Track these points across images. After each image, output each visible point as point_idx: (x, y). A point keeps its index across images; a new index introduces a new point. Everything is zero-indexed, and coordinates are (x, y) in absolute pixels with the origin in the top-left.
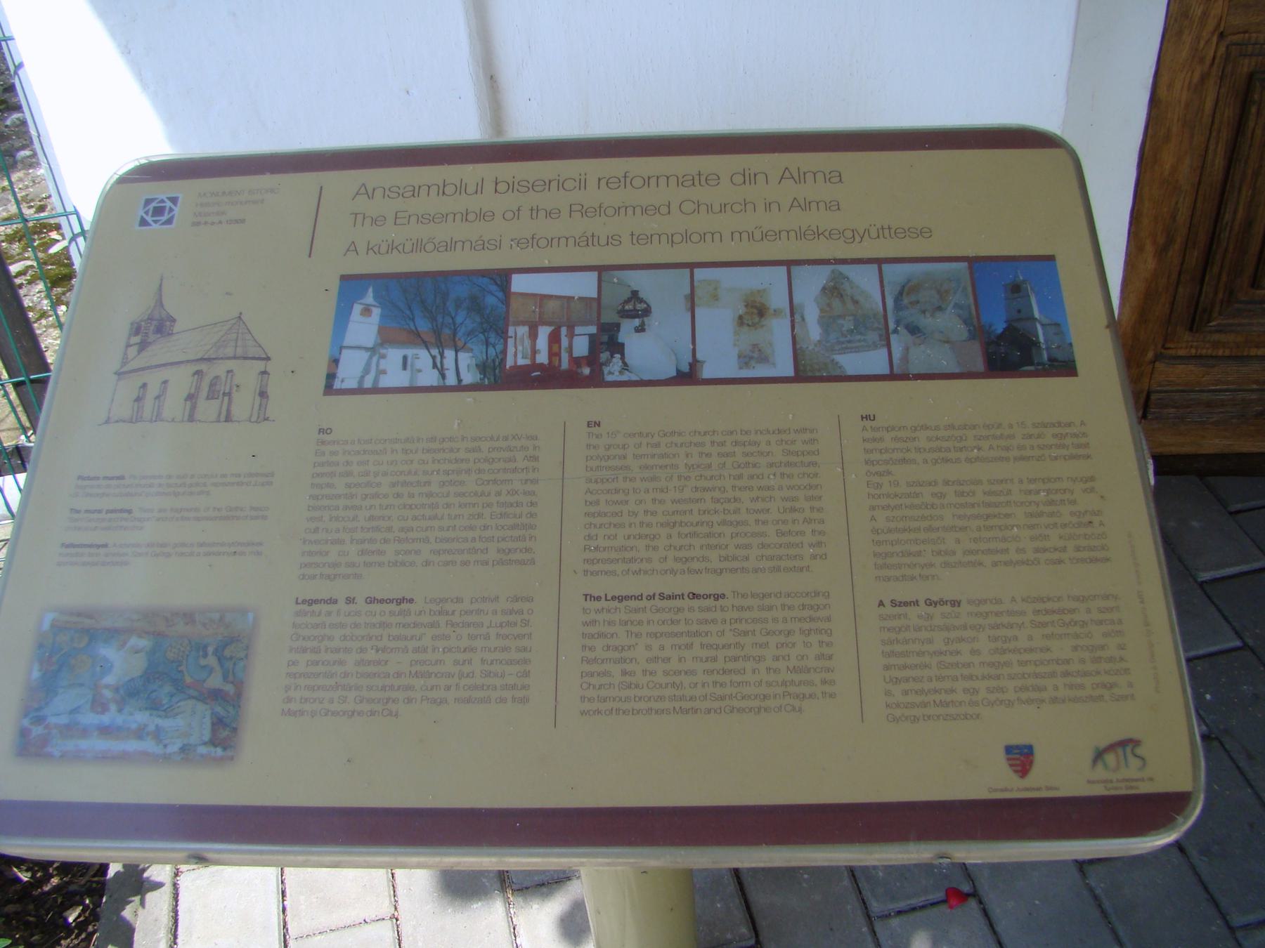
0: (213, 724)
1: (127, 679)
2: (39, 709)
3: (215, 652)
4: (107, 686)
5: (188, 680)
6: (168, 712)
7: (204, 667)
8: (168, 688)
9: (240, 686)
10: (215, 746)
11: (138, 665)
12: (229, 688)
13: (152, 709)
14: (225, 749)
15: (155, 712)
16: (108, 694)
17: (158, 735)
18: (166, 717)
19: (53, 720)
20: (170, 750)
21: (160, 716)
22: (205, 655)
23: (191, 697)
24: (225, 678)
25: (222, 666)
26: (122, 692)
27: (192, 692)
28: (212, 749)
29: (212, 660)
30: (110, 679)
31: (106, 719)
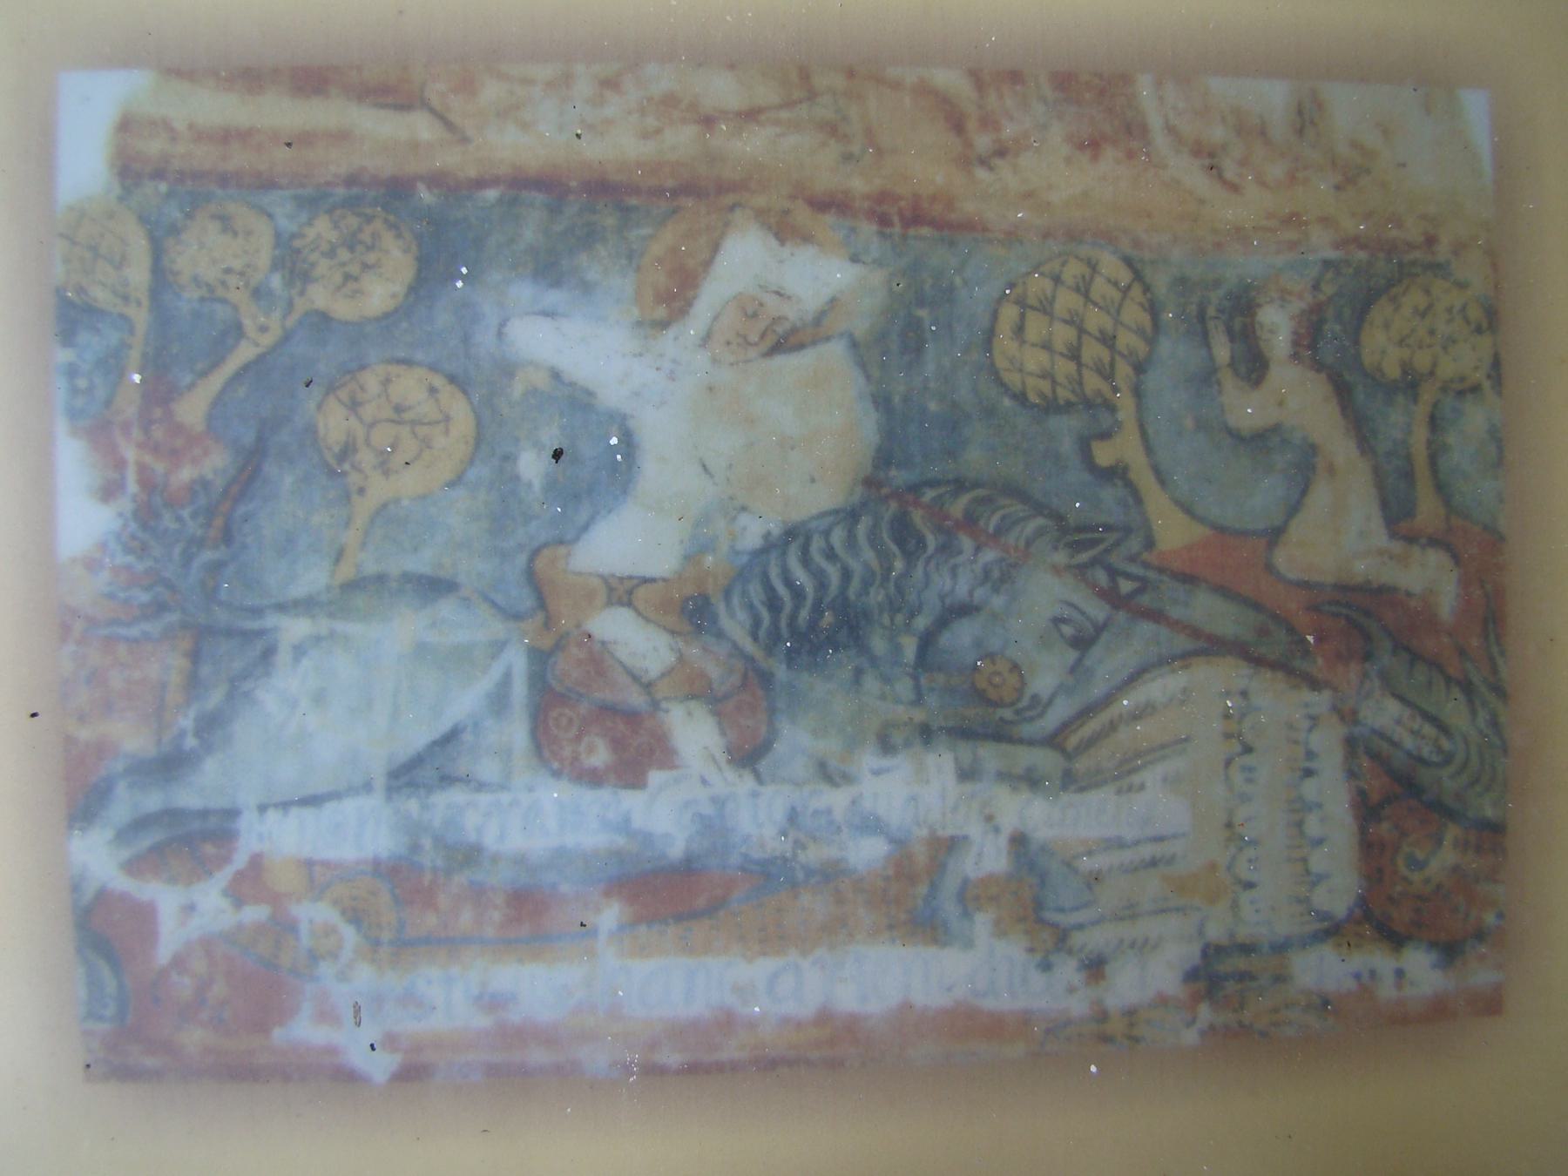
1: (753, 531)
3: (1309, 339)
4: (623, 591)
5: (1173, 532)
7: (1260, 442)
9: (1483, 553)
10: (1395, 939)
12: (1430, 578)
13: (964, 733)
15: (990, 755)
16: (638, 643)
18: (1069, 781)
21: (1031, 780)
23: (1212, 646)
24: (1396, 513)
25: (1361, 428)
27: (1208, 610)
28: (1381, 960)
30: (629, 540)
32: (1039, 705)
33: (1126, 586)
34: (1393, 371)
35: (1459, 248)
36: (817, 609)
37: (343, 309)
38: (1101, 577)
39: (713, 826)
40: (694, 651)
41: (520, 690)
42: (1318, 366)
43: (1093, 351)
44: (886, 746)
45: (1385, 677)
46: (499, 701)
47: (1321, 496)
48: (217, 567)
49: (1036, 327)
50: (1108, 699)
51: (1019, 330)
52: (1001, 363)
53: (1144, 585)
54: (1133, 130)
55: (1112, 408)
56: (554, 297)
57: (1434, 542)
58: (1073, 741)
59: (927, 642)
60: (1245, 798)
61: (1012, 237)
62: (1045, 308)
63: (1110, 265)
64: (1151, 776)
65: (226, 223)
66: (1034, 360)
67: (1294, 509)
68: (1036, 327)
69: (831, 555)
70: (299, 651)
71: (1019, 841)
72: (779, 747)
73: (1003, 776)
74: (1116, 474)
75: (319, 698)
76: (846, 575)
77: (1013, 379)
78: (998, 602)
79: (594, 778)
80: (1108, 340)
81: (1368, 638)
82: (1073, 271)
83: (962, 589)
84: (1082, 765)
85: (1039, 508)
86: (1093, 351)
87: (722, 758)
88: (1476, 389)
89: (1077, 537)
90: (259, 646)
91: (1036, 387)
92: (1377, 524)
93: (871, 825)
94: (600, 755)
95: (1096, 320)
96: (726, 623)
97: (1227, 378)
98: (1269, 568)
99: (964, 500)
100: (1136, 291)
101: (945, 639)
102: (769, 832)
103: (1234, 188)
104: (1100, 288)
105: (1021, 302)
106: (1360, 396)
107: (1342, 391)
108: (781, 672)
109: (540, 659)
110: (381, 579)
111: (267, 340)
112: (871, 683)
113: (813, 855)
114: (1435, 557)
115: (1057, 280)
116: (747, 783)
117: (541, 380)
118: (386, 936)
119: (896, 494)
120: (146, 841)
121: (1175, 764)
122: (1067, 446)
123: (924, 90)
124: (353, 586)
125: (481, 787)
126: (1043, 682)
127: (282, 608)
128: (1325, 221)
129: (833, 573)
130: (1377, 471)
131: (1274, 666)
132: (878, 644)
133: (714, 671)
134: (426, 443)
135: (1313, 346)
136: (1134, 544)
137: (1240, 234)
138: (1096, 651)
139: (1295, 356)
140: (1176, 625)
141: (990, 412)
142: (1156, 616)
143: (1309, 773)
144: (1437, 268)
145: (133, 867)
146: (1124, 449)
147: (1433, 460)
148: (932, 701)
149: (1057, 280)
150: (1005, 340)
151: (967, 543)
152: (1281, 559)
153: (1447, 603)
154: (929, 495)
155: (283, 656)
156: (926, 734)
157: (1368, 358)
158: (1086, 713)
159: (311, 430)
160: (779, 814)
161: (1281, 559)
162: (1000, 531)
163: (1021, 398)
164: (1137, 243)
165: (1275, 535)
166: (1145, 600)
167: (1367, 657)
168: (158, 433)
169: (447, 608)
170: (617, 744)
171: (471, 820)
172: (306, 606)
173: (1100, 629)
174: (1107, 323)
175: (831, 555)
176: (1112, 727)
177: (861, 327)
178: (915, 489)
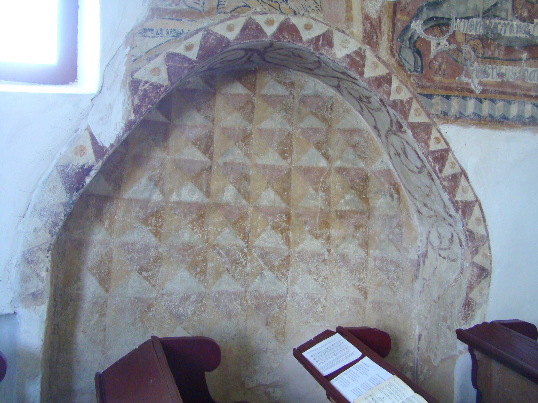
19: (459, 26)
94: (525, 14)
118: (480, 55)
120: (432, 23)
125: (502, 19)
145: (426, 31)
170: (529, 11)
171: (499, 27)
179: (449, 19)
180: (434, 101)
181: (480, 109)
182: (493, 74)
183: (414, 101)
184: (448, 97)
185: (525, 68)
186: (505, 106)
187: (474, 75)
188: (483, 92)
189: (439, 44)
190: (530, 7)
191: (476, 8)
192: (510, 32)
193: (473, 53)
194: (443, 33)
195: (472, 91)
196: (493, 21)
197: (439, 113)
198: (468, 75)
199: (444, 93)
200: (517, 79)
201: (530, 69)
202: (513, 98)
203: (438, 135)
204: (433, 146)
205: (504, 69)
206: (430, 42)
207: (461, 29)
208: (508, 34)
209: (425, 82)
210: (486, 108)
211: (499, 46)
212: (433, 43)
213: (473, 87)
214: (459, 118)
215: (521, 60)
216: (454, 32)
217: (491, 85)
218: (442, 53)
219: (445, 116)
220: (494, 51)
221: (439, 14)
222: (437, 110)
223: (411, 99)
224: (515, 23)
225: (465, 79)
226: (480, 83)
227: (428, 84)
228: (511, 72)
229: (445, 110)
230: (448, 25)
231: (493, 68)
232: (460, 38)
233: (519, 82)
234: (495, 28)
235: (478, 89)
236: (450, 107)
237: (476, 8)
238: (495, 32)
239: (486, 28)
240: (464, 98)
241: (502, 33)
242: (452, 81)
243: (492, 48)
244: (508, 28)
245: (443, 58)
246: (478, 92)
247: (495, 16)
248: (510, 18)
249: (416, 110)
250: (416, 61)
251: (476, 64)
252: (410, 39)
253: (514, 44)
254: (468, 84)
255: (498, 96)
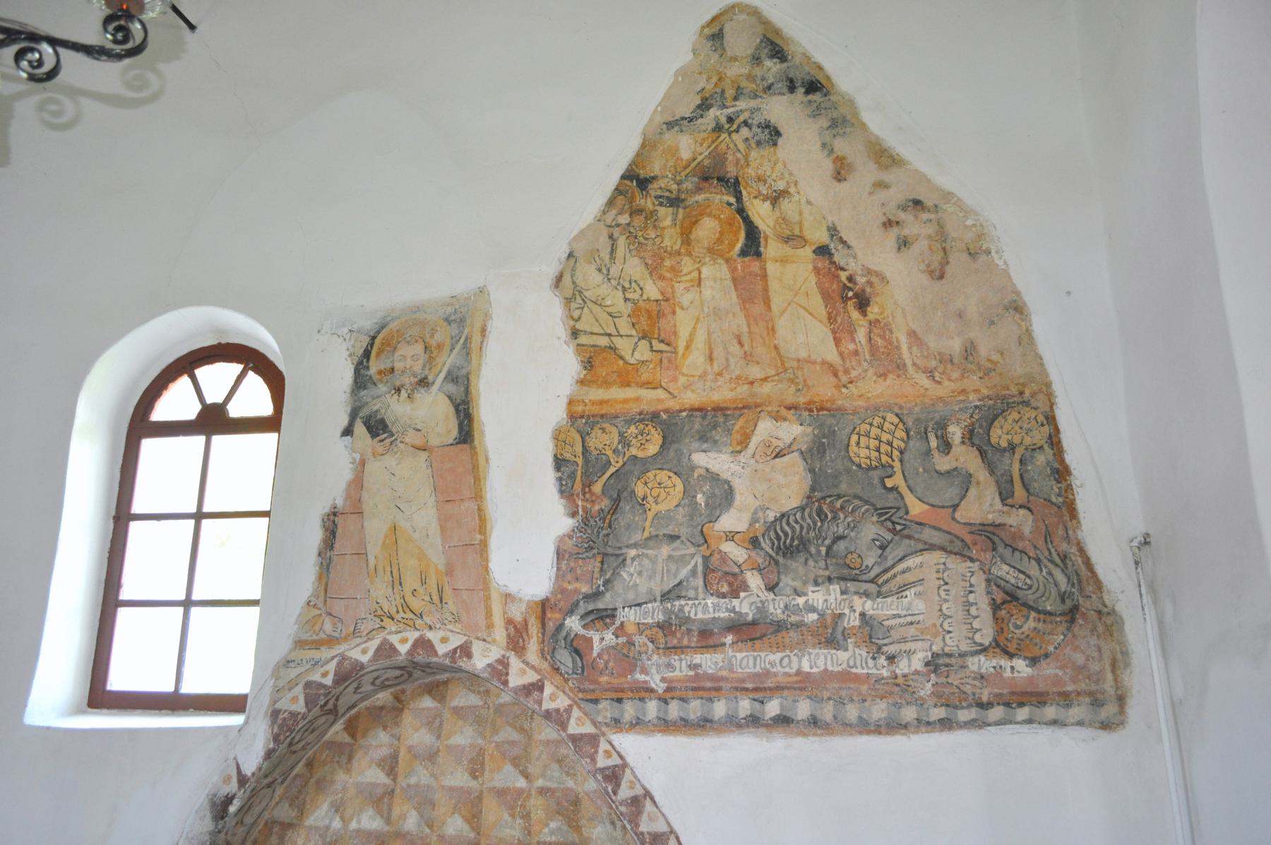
0: (996, 607)
1: (771, 516)
2: (597, 595)
3: (970, 436)
4: (730, 536)
5: (916, 508)
6: (878, 586)
8: (871, 530)
11: (788, 487)
12: (1021, 520)
13: (842, 579)
14: (1033, 661)
16: (737, 553)
17: (871, 633)
19: (629, 616)
20: (903, 667)
21: (866, 594)
22: (946, 446)
23: (932, 547)
24: (1005, 496)
26: (766, 545)
27: (929, 535)
29: (965, 457)
30: (733, 520)
31: (744, 607)
32: (869, 569)
33: (898, 528)
34: (1004, 444)
35: (1033, 395)
36: (793, 539)
37: (640, 454)
38: (889, 524)
39: (762, 609)
40: (753, 554)
41: (700, 568)
42: (973, 445)
43: (884, 448)
44: (816, 583)
45: (1002, 557)
46: (694, 572)
47: (973, 491)
48: (608, 535)
49: (863, 440)
50: (893, 566)
51: (858, 443)
52: (852, 454)
53: (905, 527)
54: (901, 367)
55: (892, 467)
56: (705, 446)
57: (1021, 507)
58: (880, 581)
59: (829, 548)
60: (946, 601)
61: (855, 412)
62: (868, 435)
63: (891, 418)
64: (910, 593)
65: (603, 429)
66: (864, 453)
67: (963, 497)
68: (863, 440)
69: (797, 522)
70: (633, 559)
71: (863, 615)
72: (781, 585)
73: (856, 593)
74: (894, 489)
75: (640, 573)
76: (802, 528)
77: (856, 460)
78: (853, 534)
79: (724, 596)
80: (890, 444)
81: (994, 543)
82: (877, 421)
83: (841, 530)
84: (884, 589)
85: (867, 502)
86: (884, 448)
87: (763, 587)
88: (1041, 448)
89: (882, 512)
90: (621, 558)
91: (864, 463)
92: (997, 500)
93: (813, 609)
94: (725, 589)
95: (885, 437)
96: (763, 545)
97: (935, 453)
98: (954, 519)
99: (840, 501)
100: (901, 425)
101: (835, 547)
102: (779, 611)
103: (939, 383)
104: (887, 426)
105: (859, 434)
106: (990, 454)
107: (982, 453)
108: (781, 560)
109: (706, 559)
110: (657, 536)
111: (619, 465)
112: (811, 563)
113: (793, 619)
114: (1022, 512)
115: (871, 425)
116: (772, 596)
117: (703, 472)
119: (818, 501)
121: (919, 588)
122: (876, 481)
123: (824, 363)
124: (647, 539)
125: (690, 599)
126: (869, 561)
127: (627, 547)
128: (976, 391)
129: (797, 527)
130: (997, 482)
131: (956, 554)
132: (813, 550)
133: (760, 561)
134: (668, 493)
135: (970, 439)
136: (901, 513)
137: (941, 399)
138: (888, 550)
139: (963, 443)
140: (918, 540)
141: (848, 471)
142: (909, 537)
143: (971, 592)
144: (1026, 403)
146: (897, 480)
147: (1022, 477)
148: (831, 568)
149: (871, 425)
150: (853, 448)
151: (842, 516)
152: (957, 515)
153: (1027, 530)
154: (828, 500)
155: (628, 561)
156: (830, 579)
157: (993, 440)
158: (886, 571)
159: (633, 491)
160: (782, 606)
161: (957, 515)
162: (853, 511)
163: (859, 466)
164: (901, 408)
165: (955, 507)
166: (906, 532)
167: (994, 549)
168: (588, 496)
169: (677, 543)
170: (730, 584)
171: (687, 609)
172: (635, 546)
173: (889, 543)
174: (890, 437)
175: (797, 522)
176: (895, 576)
177: (804, 448)
178: (824, 498)
179: (615, 609)
180: (600, 706)
181: (666, 712)
182: (681, 667)
183: (575, 709)
184: (619, 701)
185: (731, 654)
186: (702, 705)
187: (654, 670)
188: (668, 690)
189: (603, 639)
190: (731, 579)
191: (650, 591)
192: (704, 613)
193: (650, 645)
194: (607, 626)
195: (652, 691)
196: (677, 603)
197: (608, 721)
198: (645, 671)
199: (615, 695)
200: (720, 669)
201: (739, 655)
202: (714, 694)
203: (609, 747)
204: (602, 762)
205: (698, 659)
206: (591, 639)
207: (632, 618)
208: (700, 616)
209: (587, 686)
210: (674, 710)
211: (689, 631)
212: (596, 638)
213: (653, 685)
214: (638, 724)
215: (724, 644)
216: (622, 623)
217: (679, 681)
218: (609, 648)
219: (617, 724)
220: (682, 638)
221: (601, 606)
222: (605, 717)
223: (570, 706)
224: (709, 602)
225: (640, 677)
226: (663, 680)
227: (592, 687)
228: (709, 662)
229: (617, 716)
230: (614, 616)
231: (681, 660)
232: (631, 629)
233: (724, 673)
234: (681, 610)
235: (660, 687)
236: (622, 712)
237: (650, 591)
238: (681, 615)
239: (667, 612)
240: (642, 699)
241: (692, 615)
242: (623, 680)
243: (679, 635)
244: (700, 608)
245: (609, 653)
246: (660, 691)
247: (679, 597)
248: (701, 596)
249: (579, 719)
250: (574, 662)
251: (655, 657)
252: (565, 639)
253: (711, 627)
254: (646, 682)
255: (691, 693)
